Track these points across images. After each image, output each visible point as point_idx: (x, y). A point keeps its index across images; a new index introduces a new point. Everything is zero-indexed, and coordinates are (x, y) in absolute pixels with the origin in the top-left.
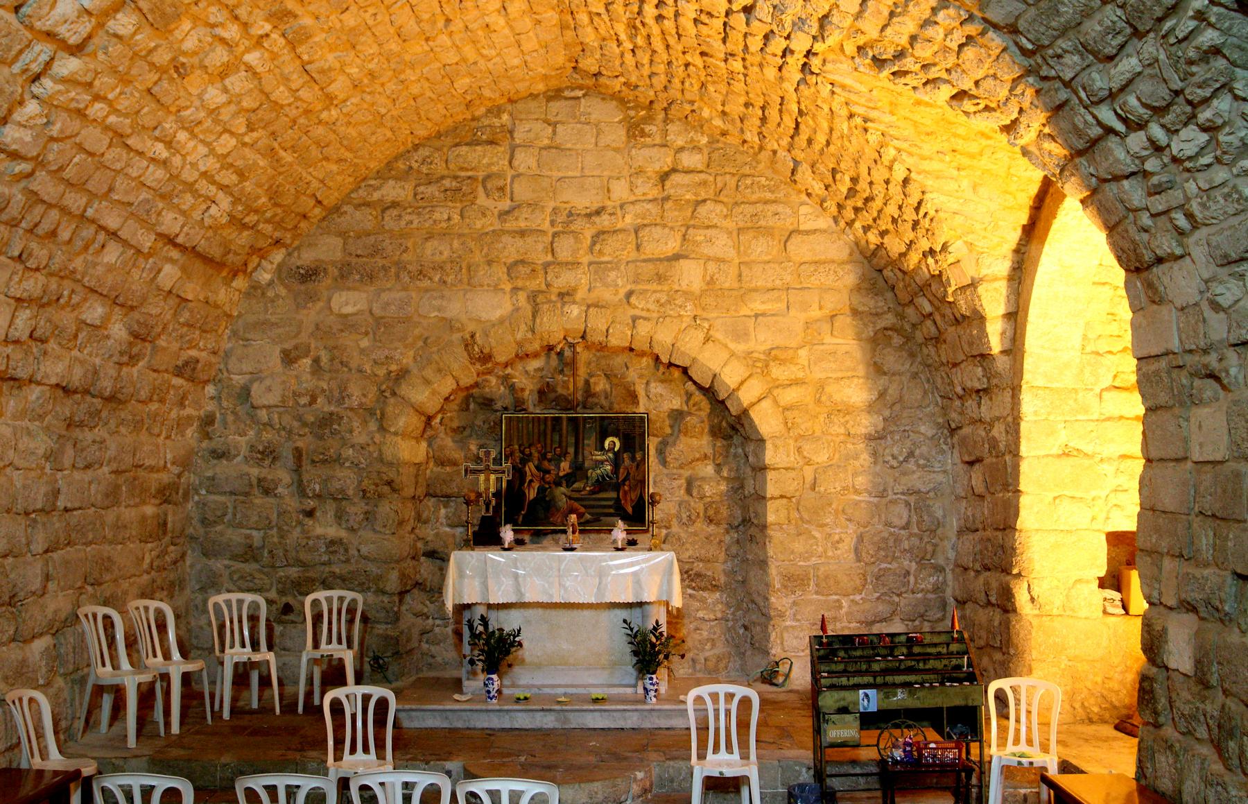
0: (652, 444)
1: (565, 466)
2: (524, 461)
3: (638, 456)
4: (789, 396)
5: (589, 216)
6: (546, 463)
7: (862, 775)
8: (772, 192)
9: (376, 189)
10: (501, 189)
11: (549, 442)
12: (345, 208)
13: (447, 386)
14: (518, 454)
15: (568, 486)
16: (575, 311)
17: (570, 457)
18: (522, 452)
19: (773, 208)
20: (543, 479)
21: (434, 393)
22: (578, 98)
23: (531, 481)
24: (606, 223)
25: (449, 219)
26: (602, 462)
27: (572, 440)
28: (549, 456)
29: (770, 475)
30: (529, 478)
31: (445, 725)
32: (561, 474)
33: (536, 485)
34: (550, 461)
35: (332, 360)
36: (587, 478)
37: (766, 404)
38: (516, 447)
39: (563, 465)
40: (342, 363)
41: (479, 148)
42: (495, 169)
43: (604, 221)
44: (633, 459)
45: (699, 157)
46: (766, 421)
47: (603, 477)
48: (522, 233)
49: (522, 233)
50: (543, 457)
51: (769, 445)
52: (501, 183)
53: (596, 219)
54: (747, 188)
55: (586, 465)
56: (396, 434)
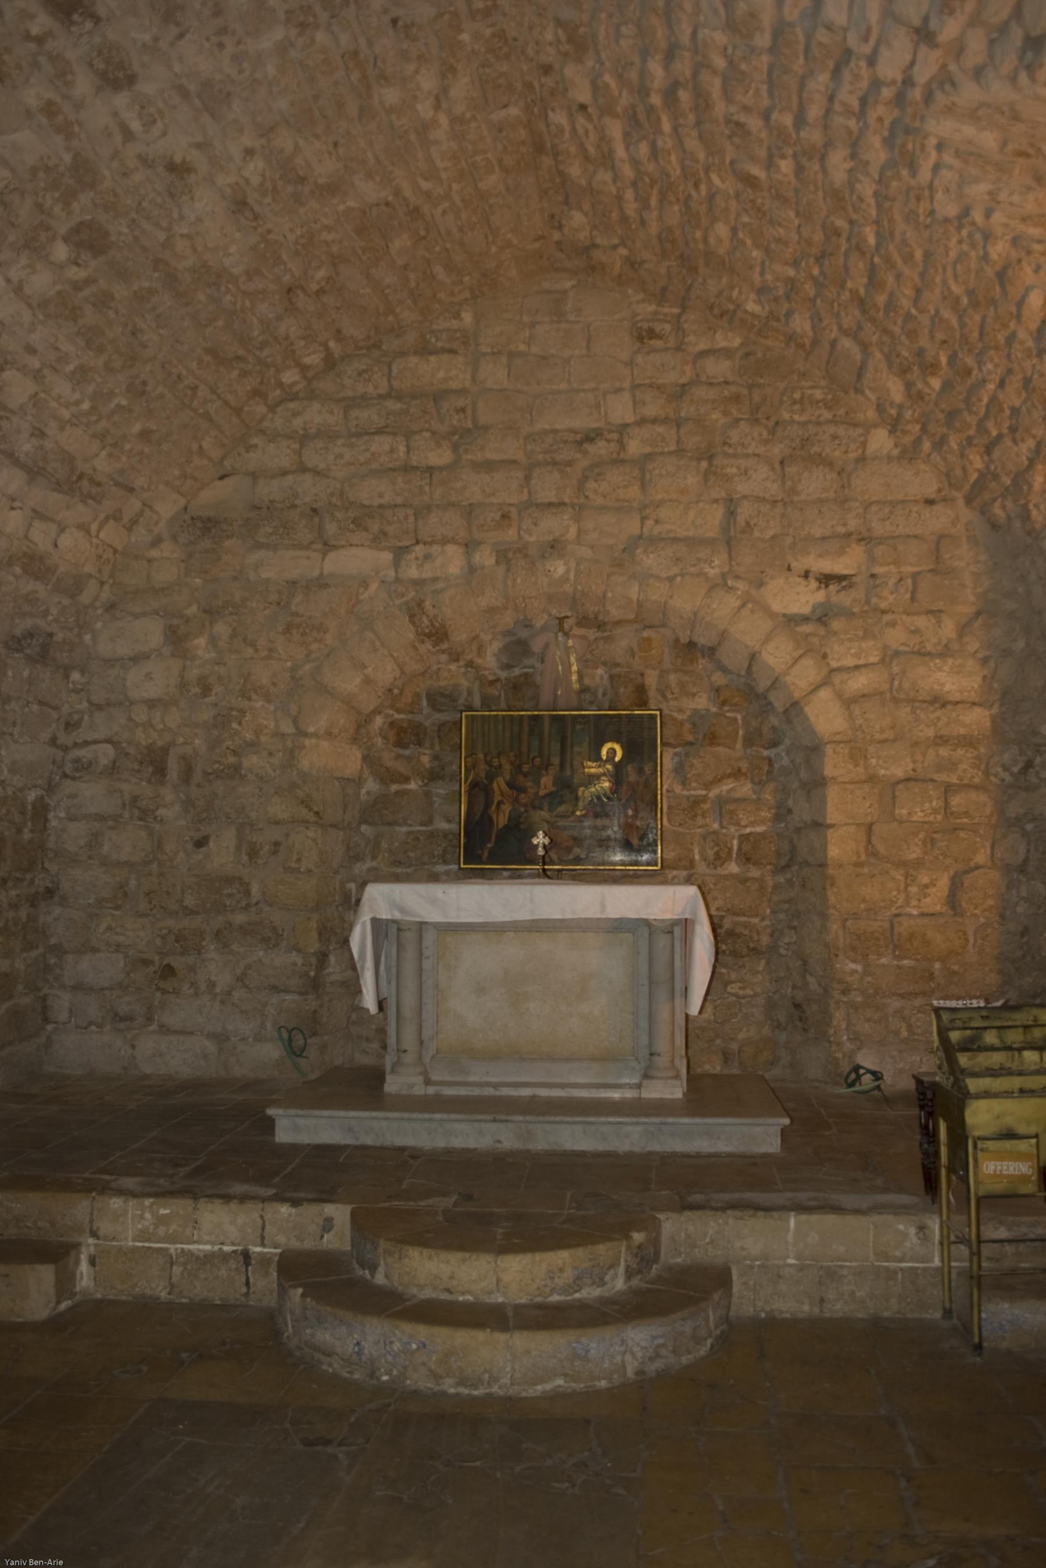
0: (667, 759)
1: (547, 782)
2: (491, 777)
3: (647, 769)
4: (859, 682)
5: (580, 443)
6: (521, 778)
7: (1009, 1241)
8: (829, 408)
9: (295, 414)
10: (463, 410)
11: (524, 749)
12: (255, 440)
13: (386, 673)
14: (482, 767)
15: (550, 810)
16: (559, 568)
17: (553, 771)
18: (489, 763)
19: (831, 429)
20: (516, 800)
21: (368, 681)
22: (565, 292)
23: (500, 803)
24: (603, 452)
25: (392, 451)
26: (597, 777)
27: (556, 747)
28: (526, 768)
29: (832, 793)
30: (497, 798)
31: (349, 1141)
32: (542, 793)
33: (507, 808)
34: (526, 775)
35: (232, 637)
36: (577, 799)
37: (824, 694)
38: (481, 756)
39: (544, 780)
40: (245, 640)
41: (432, 358)
42: (454, 385)
43: (601, 449)
44: (640, 771)
45: (728, 363)
46: (825, 716)
47: (599, 798)
48: (488, 466)
49: (488, 466)
50: (518, 769)
51: (829, 750)
52: (460, 403)
53: (591, 448)
54: (795, 402)
55: (576, 781)
56: (315, 735)
